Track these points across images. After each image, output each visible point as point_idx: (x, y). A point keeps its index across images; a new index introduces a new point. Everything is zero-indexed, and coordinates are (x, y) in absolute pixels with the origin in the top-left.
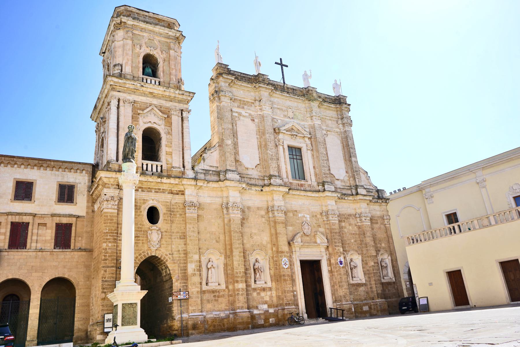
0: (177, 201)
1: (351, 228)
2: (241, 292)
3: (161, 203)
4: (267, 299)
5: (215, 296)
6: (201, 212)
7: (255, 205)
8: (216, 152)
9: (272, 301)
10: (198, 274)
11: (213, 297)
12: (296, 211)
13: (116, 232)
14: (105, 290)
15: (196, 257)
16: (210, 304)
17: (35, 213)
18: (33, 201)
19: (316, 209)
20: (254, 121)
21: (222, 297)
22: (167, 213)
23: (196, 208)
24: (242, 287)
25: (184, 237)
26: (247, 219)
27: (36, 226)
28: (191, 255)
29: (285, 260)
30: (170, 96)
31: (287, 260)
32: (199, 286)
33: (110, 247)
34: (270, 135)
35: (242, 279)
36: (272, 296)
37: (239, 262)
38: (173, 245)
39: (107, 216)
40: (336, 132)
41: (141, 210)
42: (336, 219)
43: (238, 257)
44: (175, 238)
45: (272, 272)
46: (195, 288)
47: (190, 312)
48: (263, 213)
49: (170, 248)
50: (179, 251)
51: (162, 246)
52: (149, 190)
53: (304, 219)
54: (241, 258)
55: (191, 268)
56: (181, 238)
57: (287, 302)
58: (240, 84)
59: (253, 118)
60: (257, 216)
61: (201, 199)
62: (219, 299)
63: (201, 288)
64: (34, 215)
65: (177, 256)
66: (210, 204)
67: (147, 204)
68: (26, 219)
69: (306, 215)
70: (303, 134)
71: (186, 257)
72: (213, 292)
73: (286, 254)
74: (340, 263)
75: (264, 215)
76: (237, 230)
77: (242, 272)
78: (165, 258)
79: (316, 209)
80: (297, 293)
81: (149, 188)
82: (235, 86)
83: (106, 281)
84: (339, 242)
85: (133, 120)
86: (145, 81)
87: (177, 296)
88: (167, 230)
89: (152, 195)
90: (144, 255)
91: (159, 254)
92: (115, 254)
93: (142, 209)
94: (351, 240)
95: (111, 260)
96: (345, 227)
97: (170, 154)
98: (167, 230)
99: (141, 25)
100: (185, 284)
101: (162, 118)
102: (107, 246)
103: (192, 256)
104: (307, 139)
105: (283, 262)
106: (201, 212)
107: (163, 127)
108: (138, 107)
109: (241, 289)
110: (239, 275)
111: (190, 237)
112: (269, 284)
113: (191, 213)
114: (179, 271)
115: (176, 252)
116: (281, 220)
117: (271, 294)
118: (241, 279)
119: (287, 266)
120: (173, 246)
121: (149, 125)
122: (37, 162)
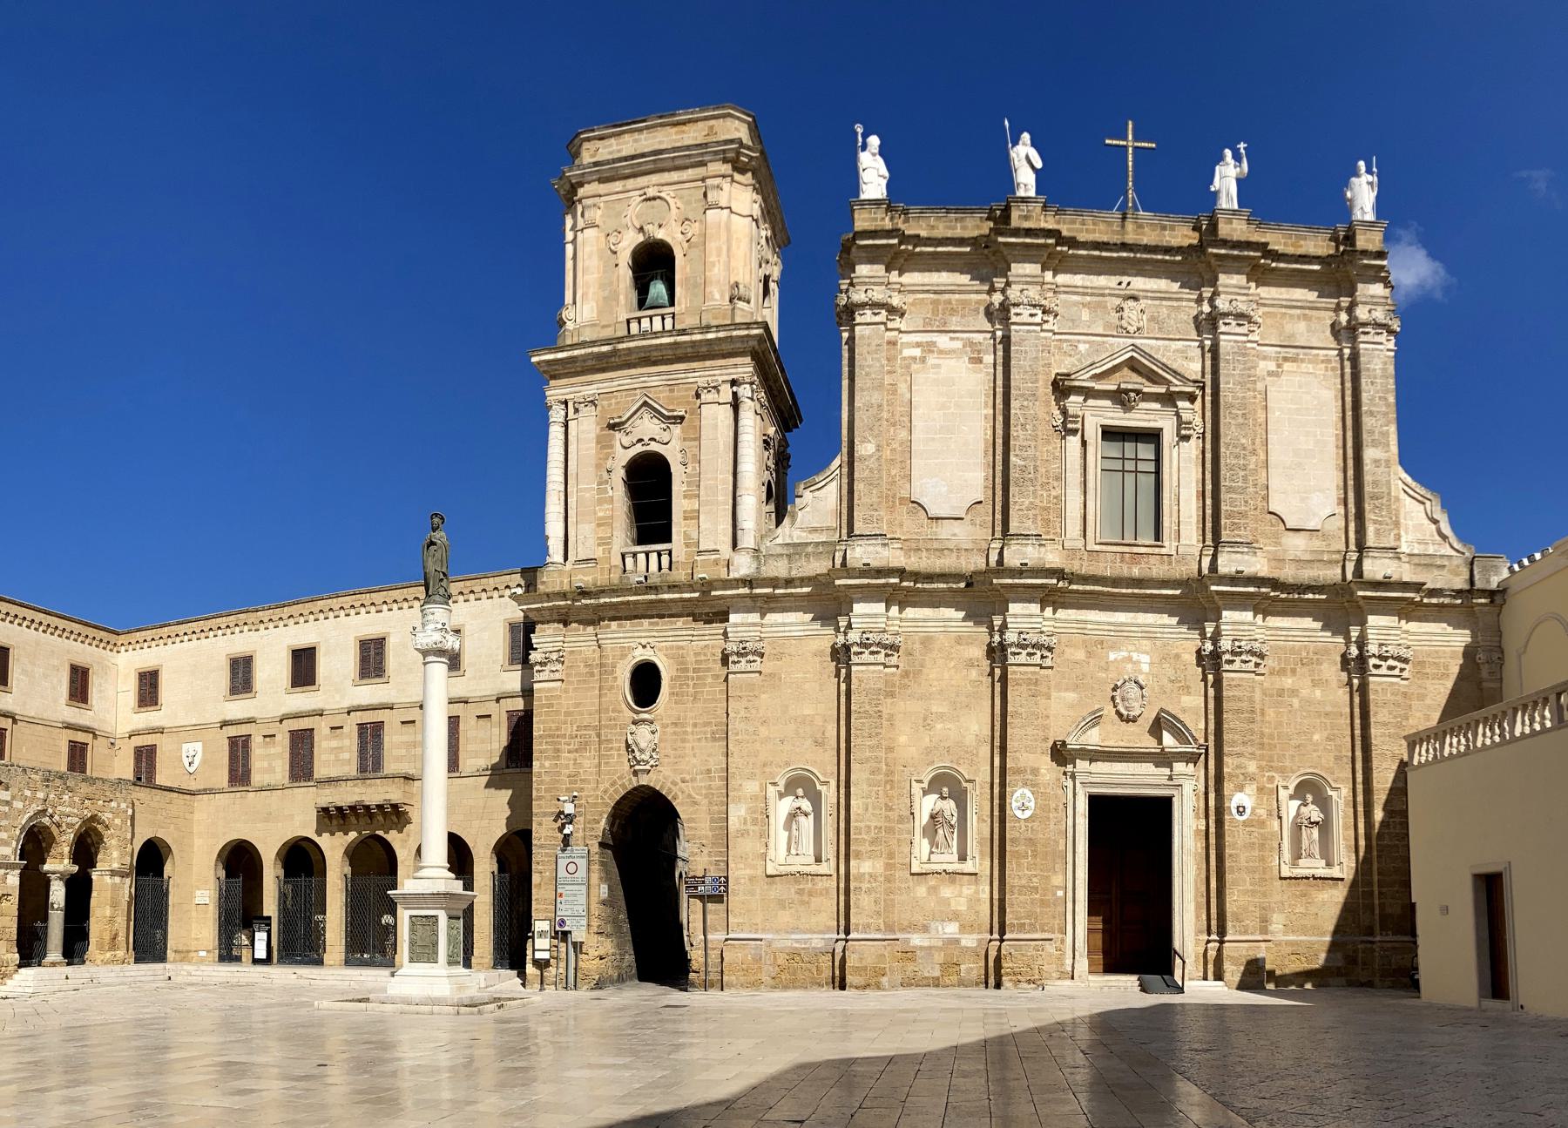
5: (800, 892)
21: (821, 894)
22: (680, 677)
29: (1023, 795)
31: (1029, 794)
35: (873, 848)
36: (979, 900)
50: (709, 771)
53: (1129, 666)
55: (738, 813)
56: (714, 739)
57: (1015, 922)
62: (813, 899)
65: (703, 784)
67: (630, 657)
69: (1135, 656)
74: (1238, 811)
78: (670, 790)
87: (696, 888)
90: (623, 785)
91: (657, 781)
93: (618, 672)
94: (1313, 733)
95: (549, 798)
105: (1016, 801)
109: (867, 876)
110: (866, 837)
117: (977, 892)
118: (869, 849)
119: (1028, 814)
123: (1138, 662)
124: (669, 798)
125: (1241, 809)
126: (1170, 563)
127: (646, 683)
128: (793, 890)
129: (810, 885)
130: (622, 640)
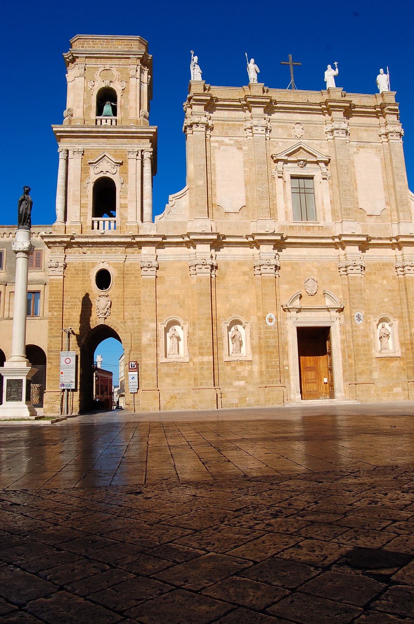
1: (385, 282)
2: (207, 366)
4: (246, 374)
6: (159, 273)
12: (297, 264)
15: (153, 325)
16: (169, 378)
20: (242, 149)
22: (119, 276)
26: (223, 278)
28: (147, 323)
33: (56, 316)
37: (206, 331)
38: (126, 312)
39: (52, 284)
40: (375, 148)
41: (89, 275)
43: (204, 325)
49: (122, 316)
50: (133, 318)
54: (209, 326)
56: (135, 305)
60: (238, 273)
66: (173, 262)
67: (96, 267)
76: (204, 292)
80: (289, 368)
83: (51, 351)
86: (99, 123)
88: (119, 295)
93: (91, 273)
96: (376, 282)
97: (125, 206)
98: (119, 295)
100: (139, 355)
103: (148, 325)
104: (322, 165)
108: (89, 155)
111: (146, 303)
112: (250, 358)
115: (130, 319)
116: (269, 277)
117: (252, 368)
120: (126, 314)
121: (102, 175)
128: (172, 369)
129: (179, 367)
130: (93, 259)
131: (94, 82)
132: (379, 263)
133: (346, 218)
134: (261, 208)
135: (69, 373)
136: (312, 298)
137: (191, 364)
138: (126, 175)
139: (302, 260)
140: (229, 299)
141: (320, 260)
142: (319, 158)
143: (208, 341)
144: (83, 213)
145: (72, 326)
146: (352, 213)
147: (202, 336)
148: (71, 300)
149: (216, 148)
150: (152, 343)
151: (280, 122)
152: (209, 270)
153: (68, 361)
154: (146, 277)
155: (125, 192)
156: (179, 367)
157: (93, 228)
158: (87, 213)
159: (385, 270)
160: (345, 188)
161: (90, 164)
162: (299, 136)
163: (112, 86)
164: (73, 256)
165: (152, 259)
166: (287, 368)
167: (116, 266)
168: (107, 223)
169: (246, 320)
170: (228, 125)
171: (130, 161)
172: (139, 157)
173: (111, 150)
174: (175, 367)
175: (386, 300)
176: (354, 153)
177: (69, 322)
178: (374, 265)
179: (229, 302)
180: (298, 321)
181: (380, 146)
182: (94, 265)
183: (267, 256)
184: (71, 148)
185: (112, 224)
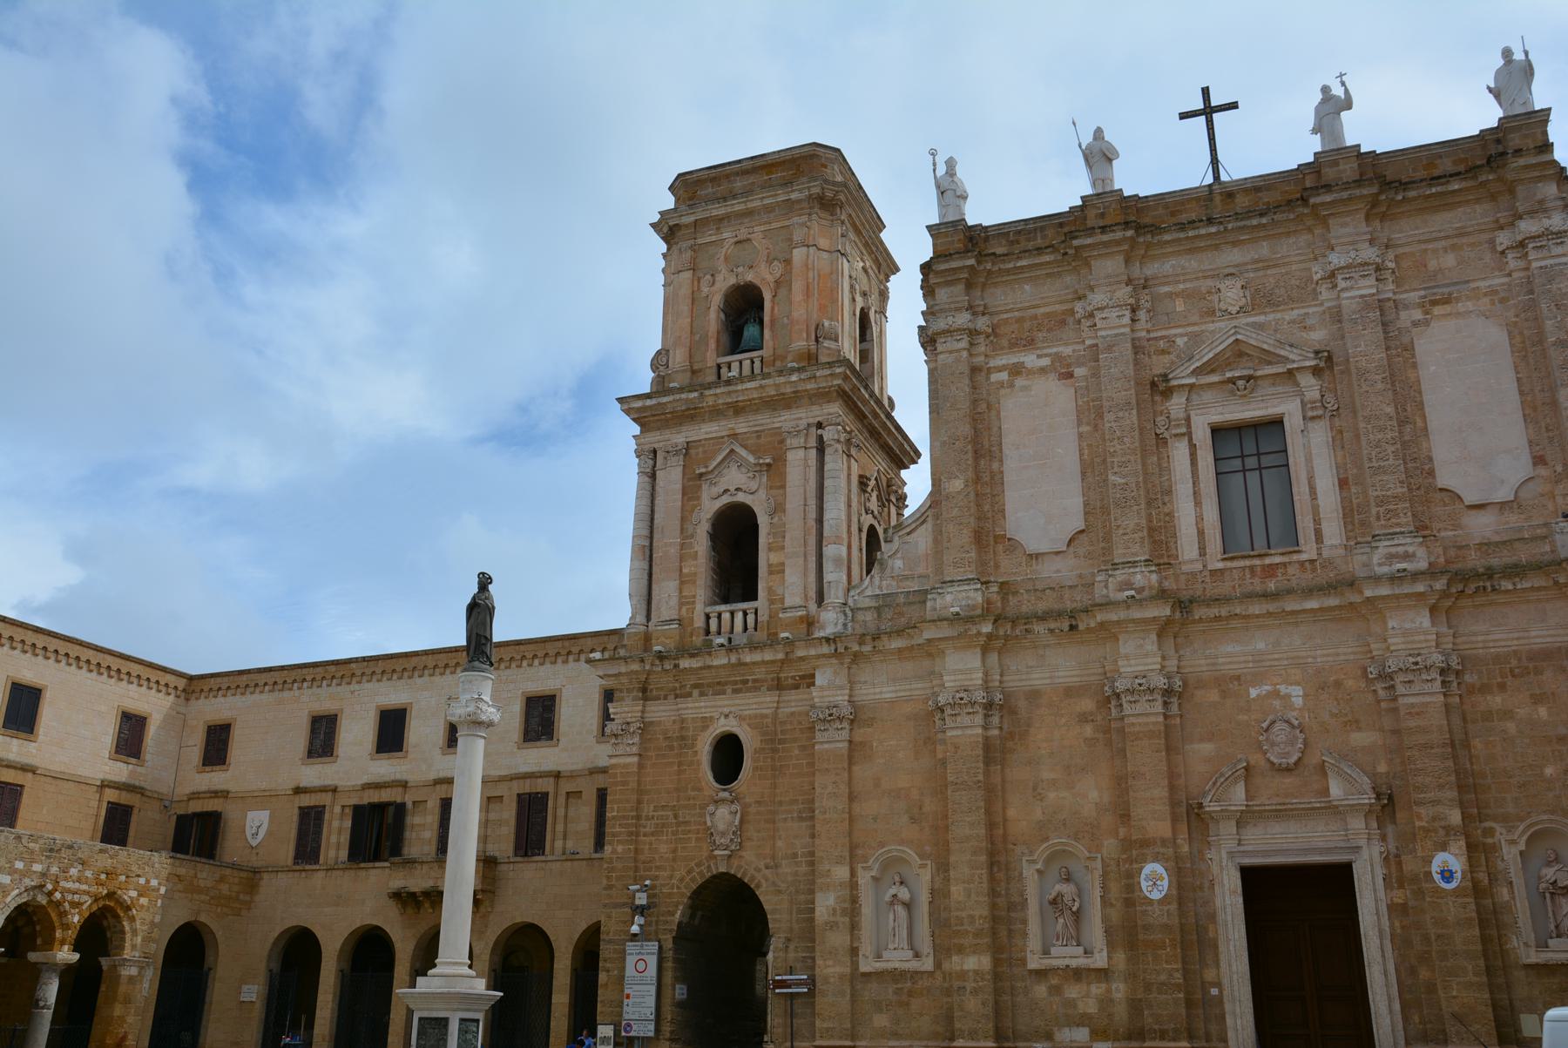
0: (793, 709)
1: (1543, 712)
3: (748, 721)
4: (1091, 1007)
5: (898, 992)
6: (860, 734)
7: (1057, 681)
8: (924, 526)
9: (1110, 1015)
10: (843, 923)
11: (895, 993)
12: (1238, 678)
13: (635, 813)
14: (608, 965)
15: (842, 873)
17: (559, 769)
18: (555, 739)
19: (1338, 655)
22: (764, 749)
23: (846, 724)
24: (976, 968)
25: (808, 815)
27: (562, 800)
30: (783, 394)
32: (847, 960)
34: (1121, 414)
35: (979, 941)
36: (1111, 1000)
38: (780, 839)
40: (1485, 295)
41: (695, 749)
42: (1427, 687)
44: (785, 819)
45: (1115, 915)
46: (834, 966)
47: (818, 1035)
48: (1087, 704)
50: (795, 855)
51: (747, 844)
52: (718, 688)
53: (1277, 703)
55: (826, 904)
56: (801, 819)
58: (1011, 265)
59: (1069, 365)
60: (1063, 720)
61: (865, 692)
63: (855, 965)
64: (557, 775)
65: (788, 870)
66: (892, 702)
67: (711, 729)
68: (545, 785)
69: (1283, 689)
70: (1286, 360)
71: (813, 871)
72: (897, 976)
73: (1162, 850)
74: (1443, 878)
75: (1091, 714)
77: (981, 917)
78: (753, 878)
79: (1338, 655)
80: (1221, 992)
81: (719, 683)
82: (999, 280)
84: (1441, 787)
85: (686, 498)
89: (726, 703)
92: (631, 873)
97: (777, 570)
99: (715, 213)
101: (758, 468)
102: (615, 851)
103: (829, 871)
106: (860, 734)
107: (762, 494)
109: (971, 974)
112: (1100, 960)
113: (832, 741)
114: (794, 915)
116: (1147, 724)
117: (1109, 991)
120: (780, 843)
121: (726, 499)
122: (559, 644)
123: (1288, 696)
124: (752, 886)
125: (1447, 874)
126: (1314, 570)
127: (728, 755)
128: (890, 990)
129: (909, 984)
130: (703, 710)
131: (712, 275)
132: (1514, 651)
133: (1385, 527)
134: (1121, 532)
135: (643, 997)
136: (1289, 781)
137: (938, 975)
138: (781, 491)
139: (1251, 665)
140: (1040, 794)
141: (1310, 660)
142: (1294, 361)
143: (977, 913)
144: (686, 597)
145: (656, 878)
146: (1405, 508)
147: (960, 899)
148: (655, 813)
149: (1002, 387)
150: (840, 919)
151: (1179, 282)
152: (979, 719)
153: (641, 966)
154: (826, 746)
155: (779, 533)
156: (909, 984)
157: (708, 632)
158: (694, 596)
159: (1538, 672)
160: (1380, 436)
161: (701, 475)
162: (1234, 310)
163: (750, 277)
164: (660, 704)
165: (840, 698)
166: (1215, 991)
167: (756, 723)
168: (739, 617)
169: (1090, 852)
170: (1035, 317)
171: (790, 456)
172: (813, 442)
173: (748, 435)
174: (899, 986)
175: (1549, 771)
176: (1415, 324)
177: (650, 869)
178: (1497, 659)
179: (1041, 800)
180: (1242, 848)
181: (1503, 284)
182: (706, 722)
183: (1137, 665)
184: (661, 444)
185: (751, 618)
